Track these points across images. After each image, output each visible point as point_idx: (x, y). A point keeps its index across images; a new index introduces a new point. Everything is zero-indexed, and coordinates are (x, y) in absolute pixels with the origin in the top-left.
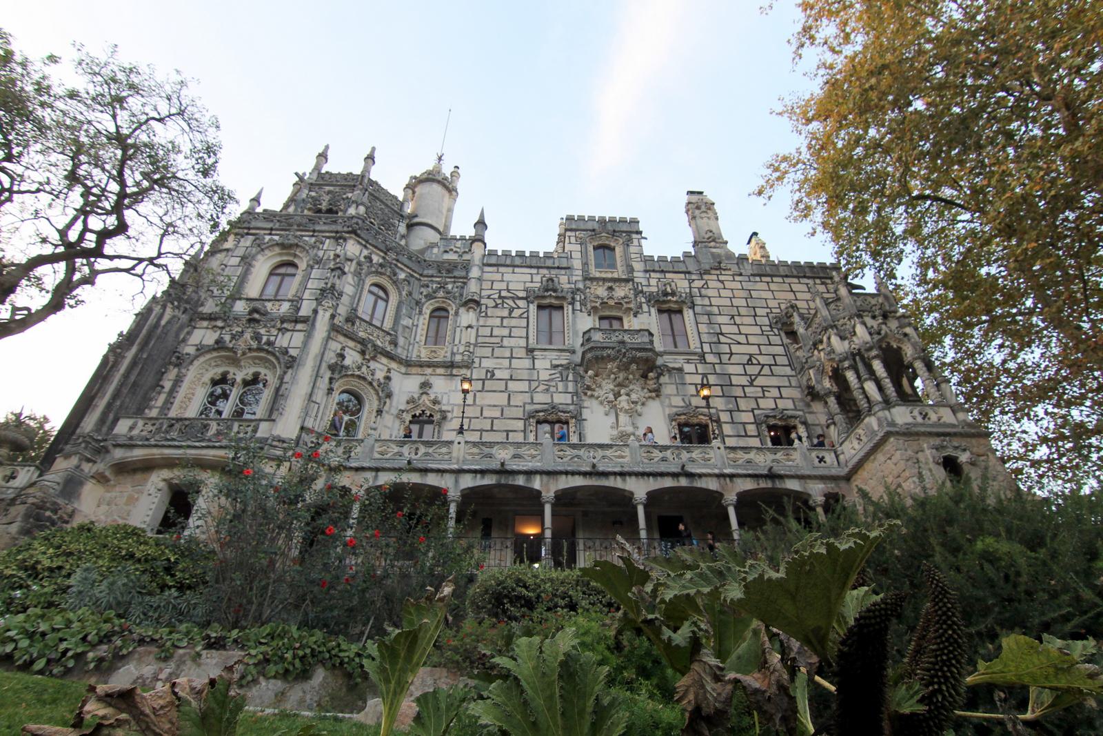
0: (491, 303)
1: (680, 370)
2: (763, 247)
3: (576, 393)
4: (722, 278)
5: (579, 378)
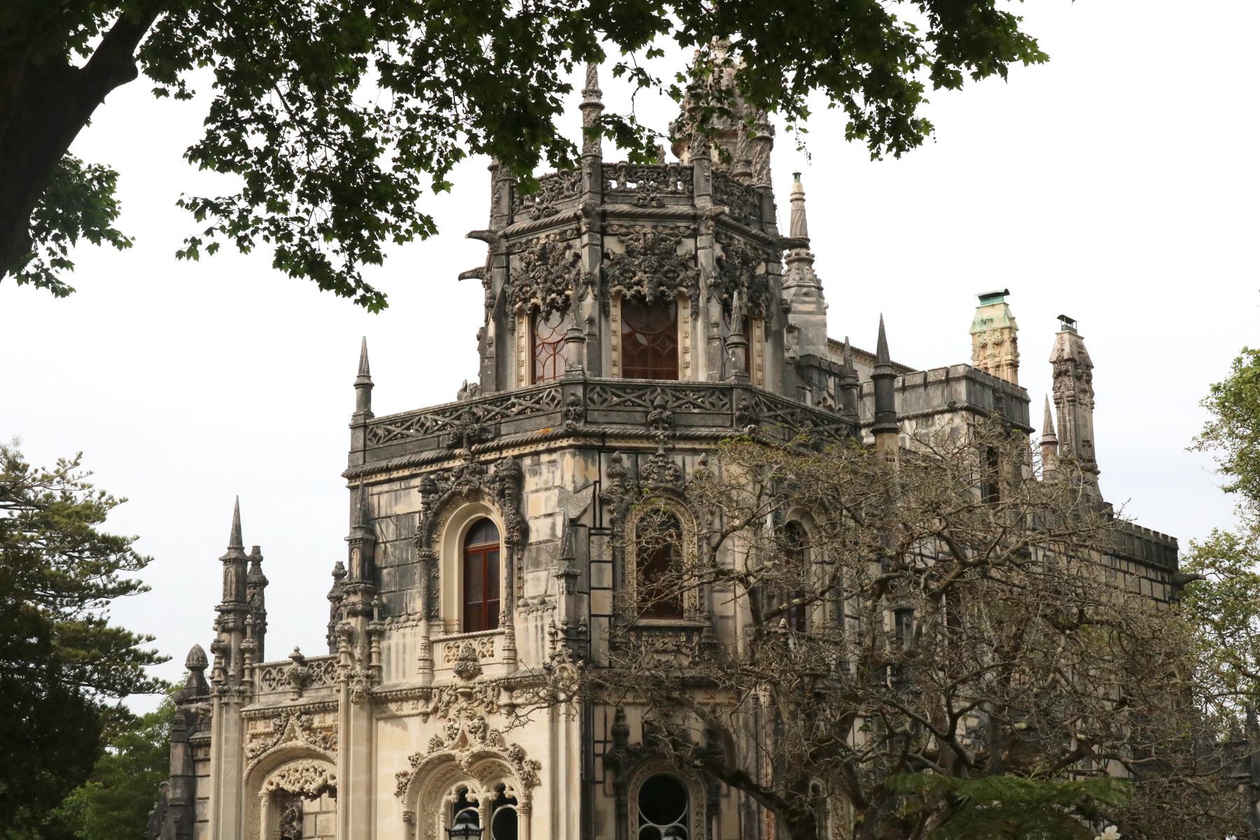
2: (1014, 341)
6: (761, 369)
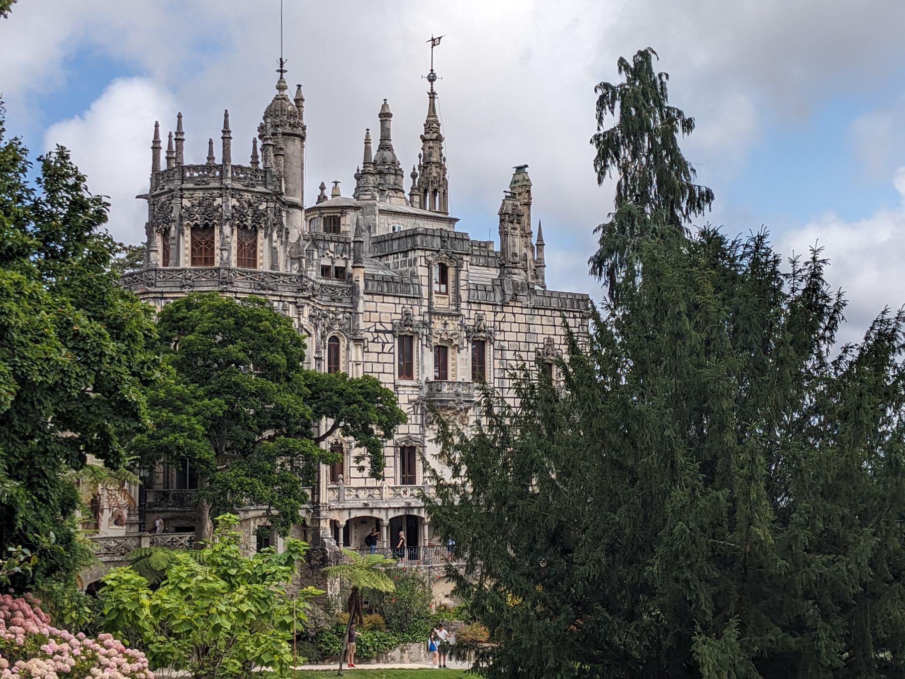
2: (529, 192)
3: (422, 425)
4: (516, 310)
6: (262, 251)
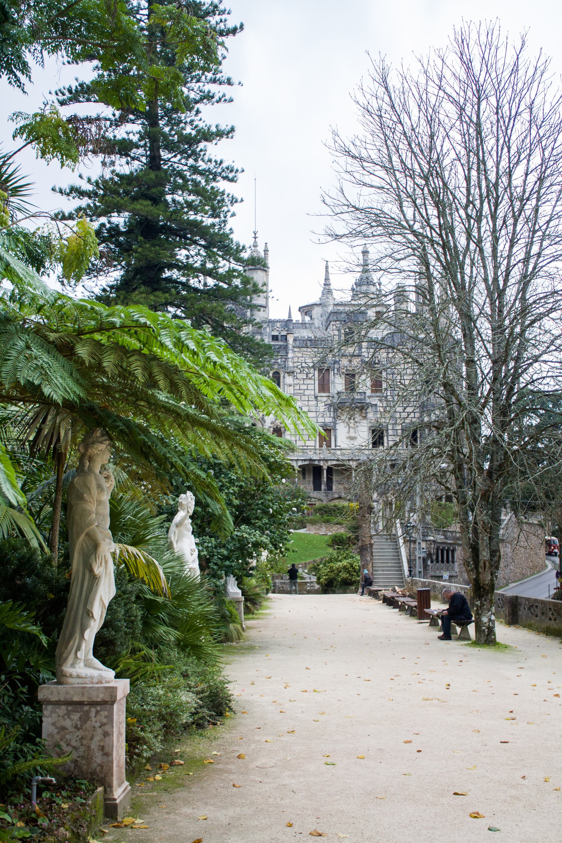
0: (298, 371)
1: (376, 405)
3: (334, 417)
5: (335, 410)
